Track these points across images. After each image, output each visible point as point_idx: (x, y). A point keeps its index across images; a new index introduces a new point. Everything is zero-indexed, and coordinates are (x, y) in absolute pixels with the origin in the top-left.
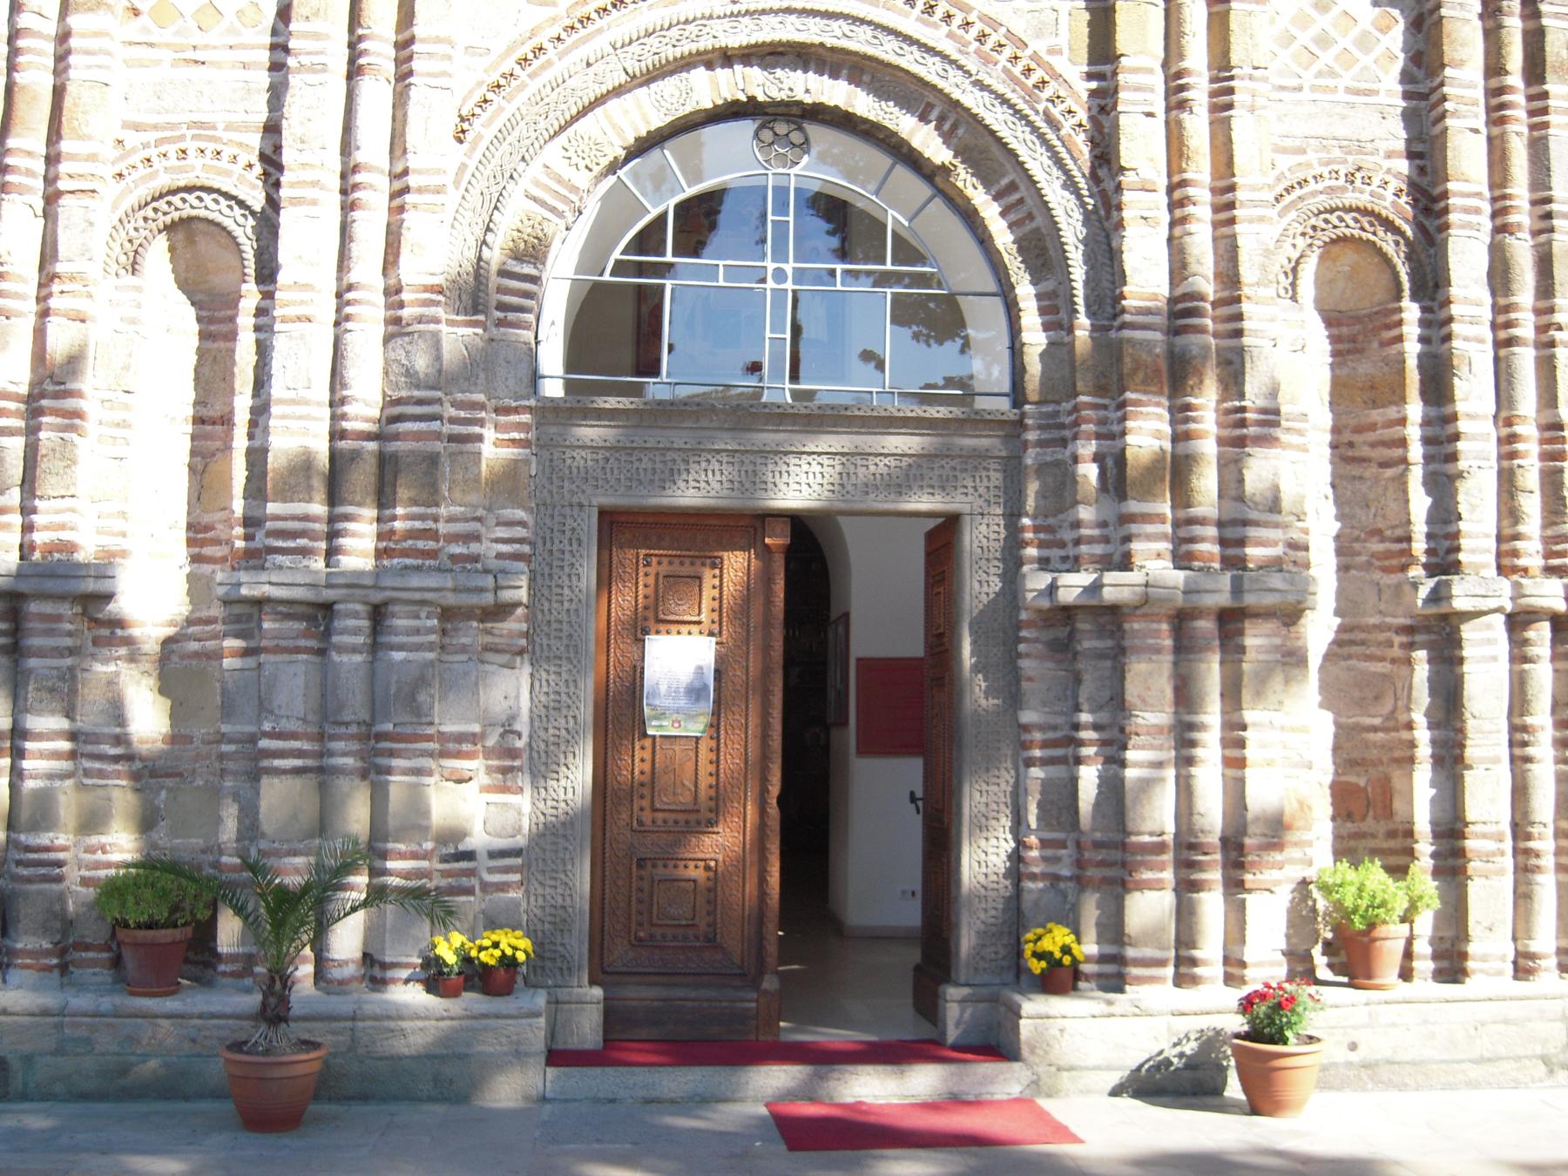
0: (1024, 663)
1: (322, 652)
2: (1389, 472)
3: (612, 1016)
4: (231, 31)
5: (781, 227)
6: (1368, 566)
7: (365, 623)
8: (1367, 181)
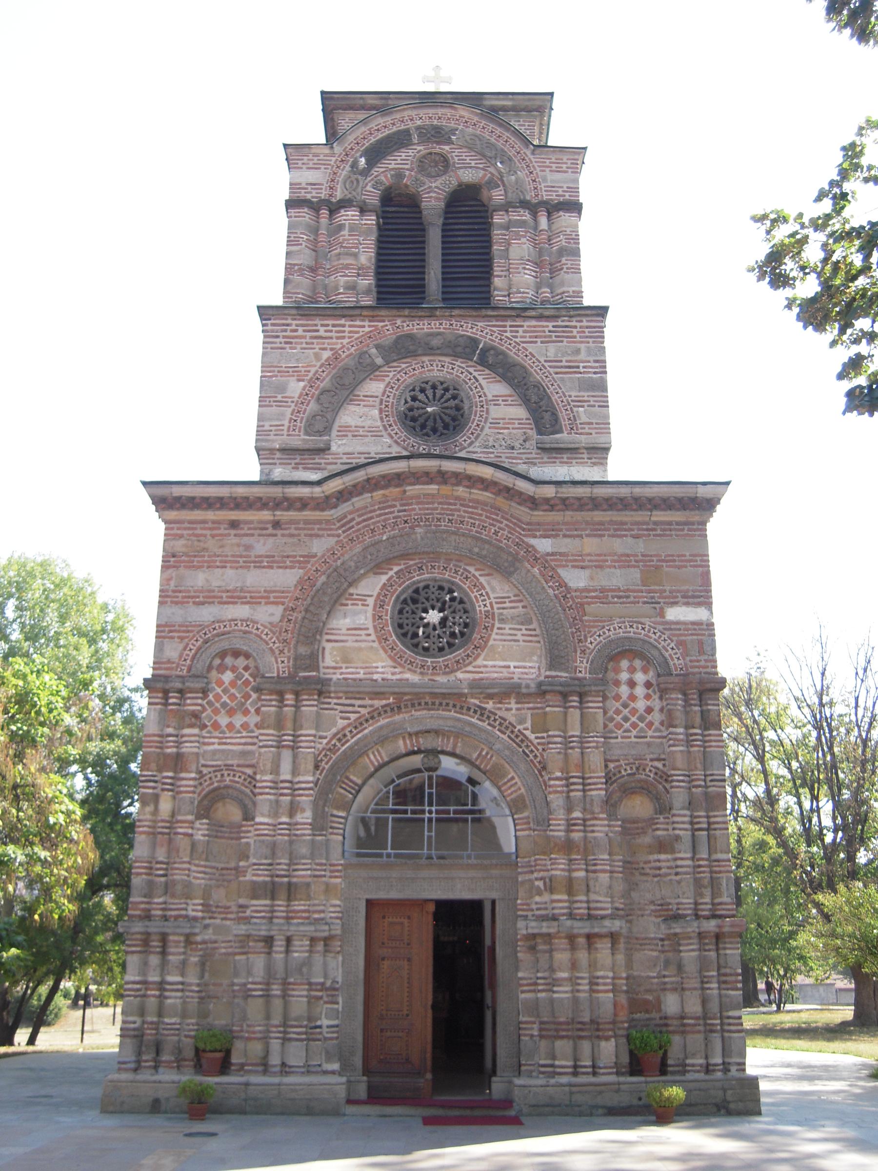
0: (519, 955)
1: (269, 953)
2: (656, 879)
3: (370, 1088)
4: (239, 732)
5: (430, 794)
6: (650, 915)
7: (284, 943)
8: (644, 770)
